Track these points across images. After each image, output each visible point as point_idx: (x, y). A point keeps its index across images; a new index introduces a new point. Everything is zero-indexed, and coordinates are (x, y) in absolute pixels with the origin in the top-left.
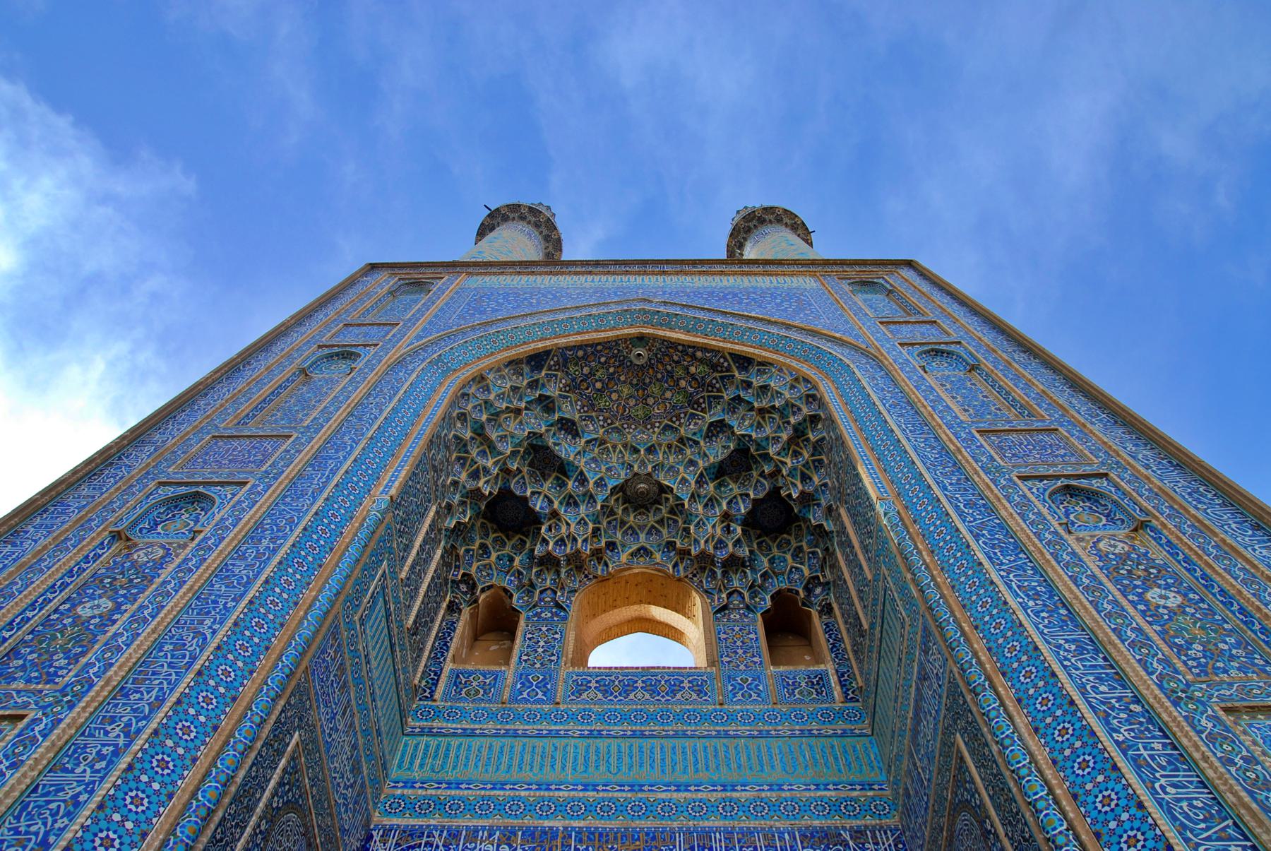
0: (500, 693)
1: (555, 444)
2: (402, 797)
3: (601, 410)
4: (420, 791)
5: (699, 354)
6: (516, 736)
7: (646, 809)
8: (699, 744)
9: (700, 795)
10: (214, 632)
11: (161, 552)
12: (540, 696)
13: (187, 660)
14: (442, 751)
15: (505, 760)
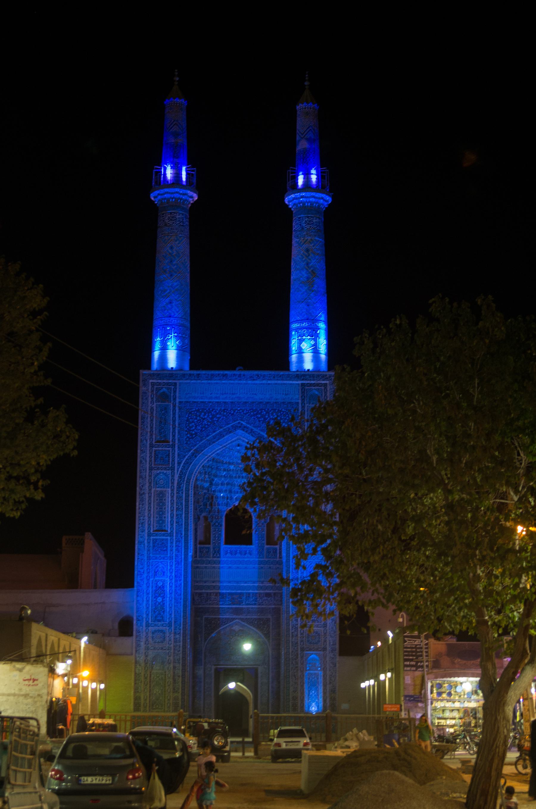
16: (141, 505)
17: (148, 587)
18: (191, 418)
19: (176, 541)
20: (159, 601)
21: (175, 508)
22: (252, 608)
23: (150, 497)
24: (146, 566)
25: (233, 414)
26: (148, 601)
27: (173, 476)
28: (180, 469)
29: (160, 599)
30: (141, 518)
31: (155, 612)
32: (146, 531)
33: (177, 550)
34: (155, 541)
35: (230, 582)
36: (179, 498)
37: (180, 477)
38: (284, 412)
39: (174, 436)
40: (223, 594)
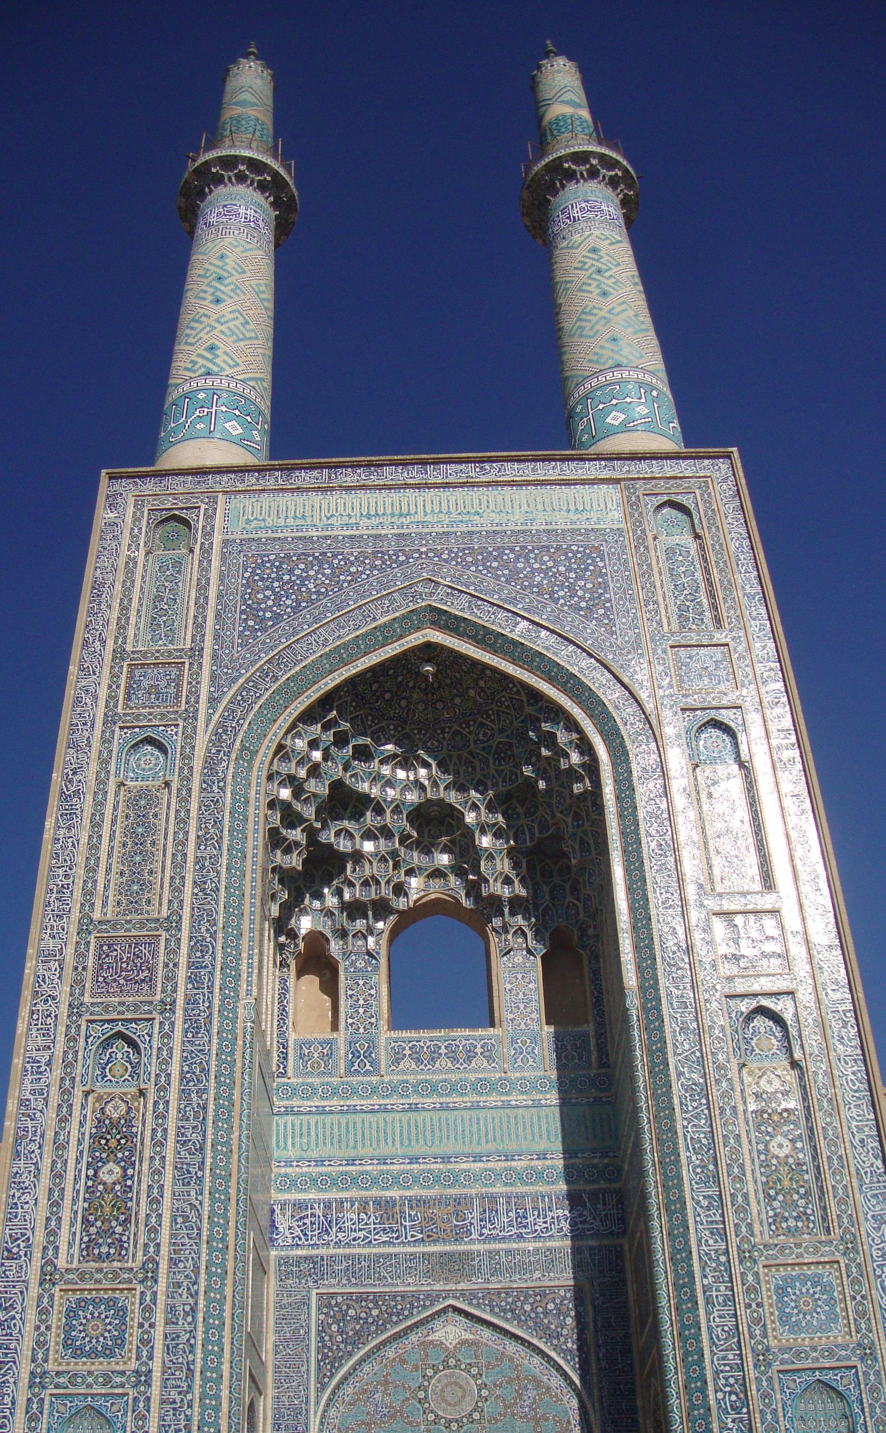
0: (336, 1066)
1: (351, 776)
2: (286, 1175)
3: (391, 719)
4: (297, 1169)
5: (488, 673)
6: (355, 1112)
7: (453, 1179)
8: (489, 1114)
9: (490, 1165)
10: (201, 1204)
11: (123, 1107)
12: (368, 1067)
13: (196, 1232)
14: (305, 1129)
15: (351, 1136)
16: (62, 832)
17: (63, 1120)
18: (262, 579)
19: (191, 949)
20: (109, 1179)
21: (192, 837)
22: (508, 1252)
23: (99, 804)
24: (61, 1039)
25: (402, 564)
26: (58, 1176)
27: (190, 737)
28: (215, 718)
29: (111, 1173)
30: (61, 872)
31: (85, 1221)
32: (76, 915)
33: (194, 980)
34: (107, 945)
35: (414, 1160)
36: (211, 806)
37: (217, 739)
38: (575, 553)
39: (199, 626)
40: (390, 1203)
